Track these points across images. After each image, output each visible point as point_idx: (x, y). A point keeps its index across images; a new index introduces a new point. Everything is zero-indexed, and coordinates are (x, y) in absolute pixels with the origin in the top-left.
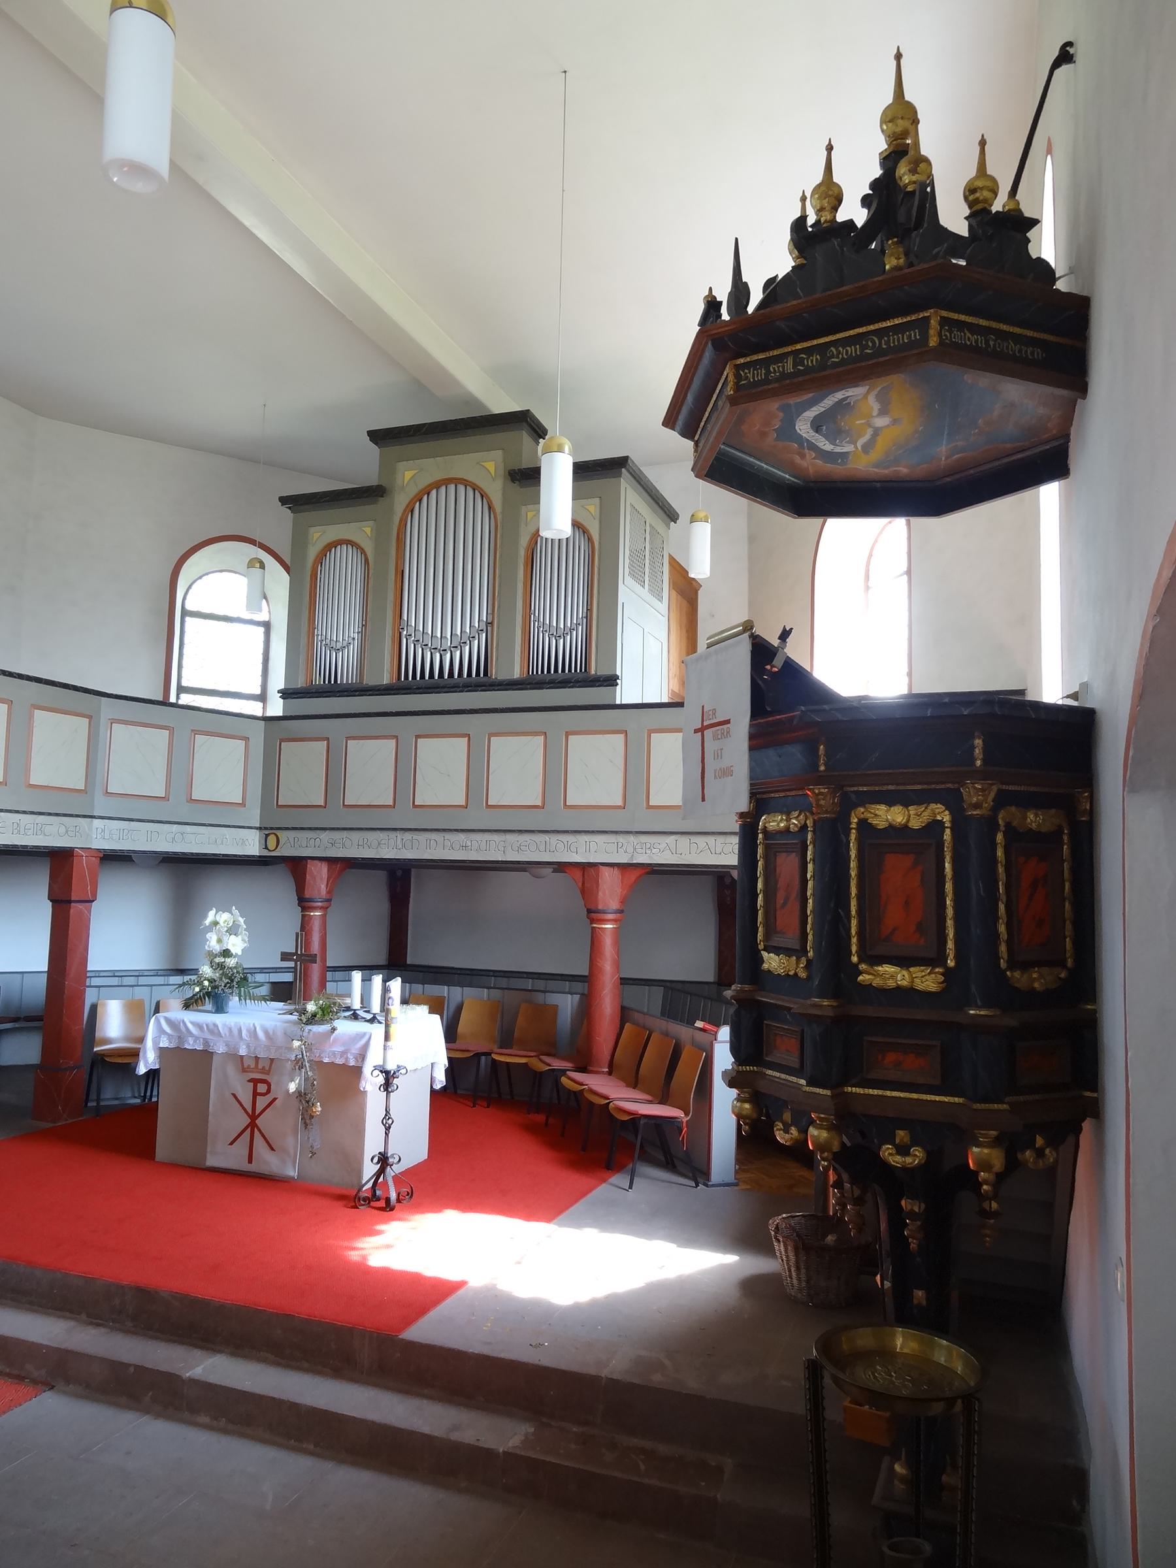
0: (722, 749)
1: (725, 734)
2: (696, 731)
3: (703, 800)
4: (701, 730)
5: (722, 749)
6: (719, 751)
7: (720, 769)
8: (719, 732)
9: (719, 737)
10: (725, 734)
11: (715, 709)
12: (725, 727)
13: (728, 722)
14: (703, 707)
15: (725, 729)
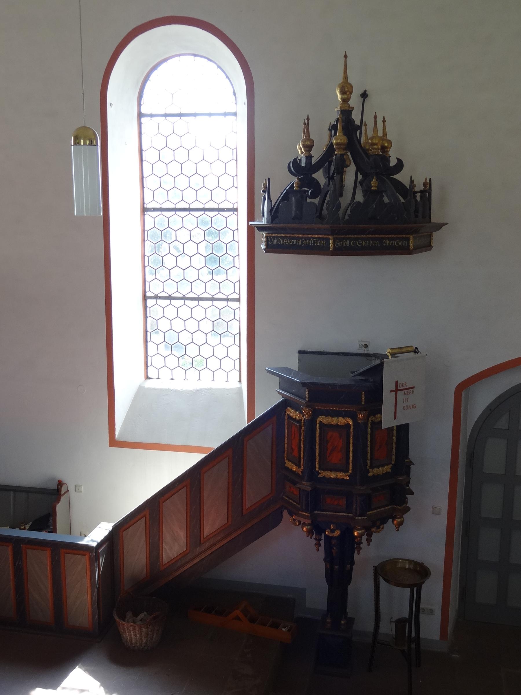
0: (408, 398)
1: (412, 392)
2: (391, 391)
3: (395, 418)
4: (396, 391)
5: (408, 398)
6: (407, 400)
7: (407, 406)
8: (409, 392)
9: (409, 393)
10: (412, 392)
11: (406, 383)
12: (411, 390)
13: (414, 387)
14: (397, 382)
15: (412, 390)
